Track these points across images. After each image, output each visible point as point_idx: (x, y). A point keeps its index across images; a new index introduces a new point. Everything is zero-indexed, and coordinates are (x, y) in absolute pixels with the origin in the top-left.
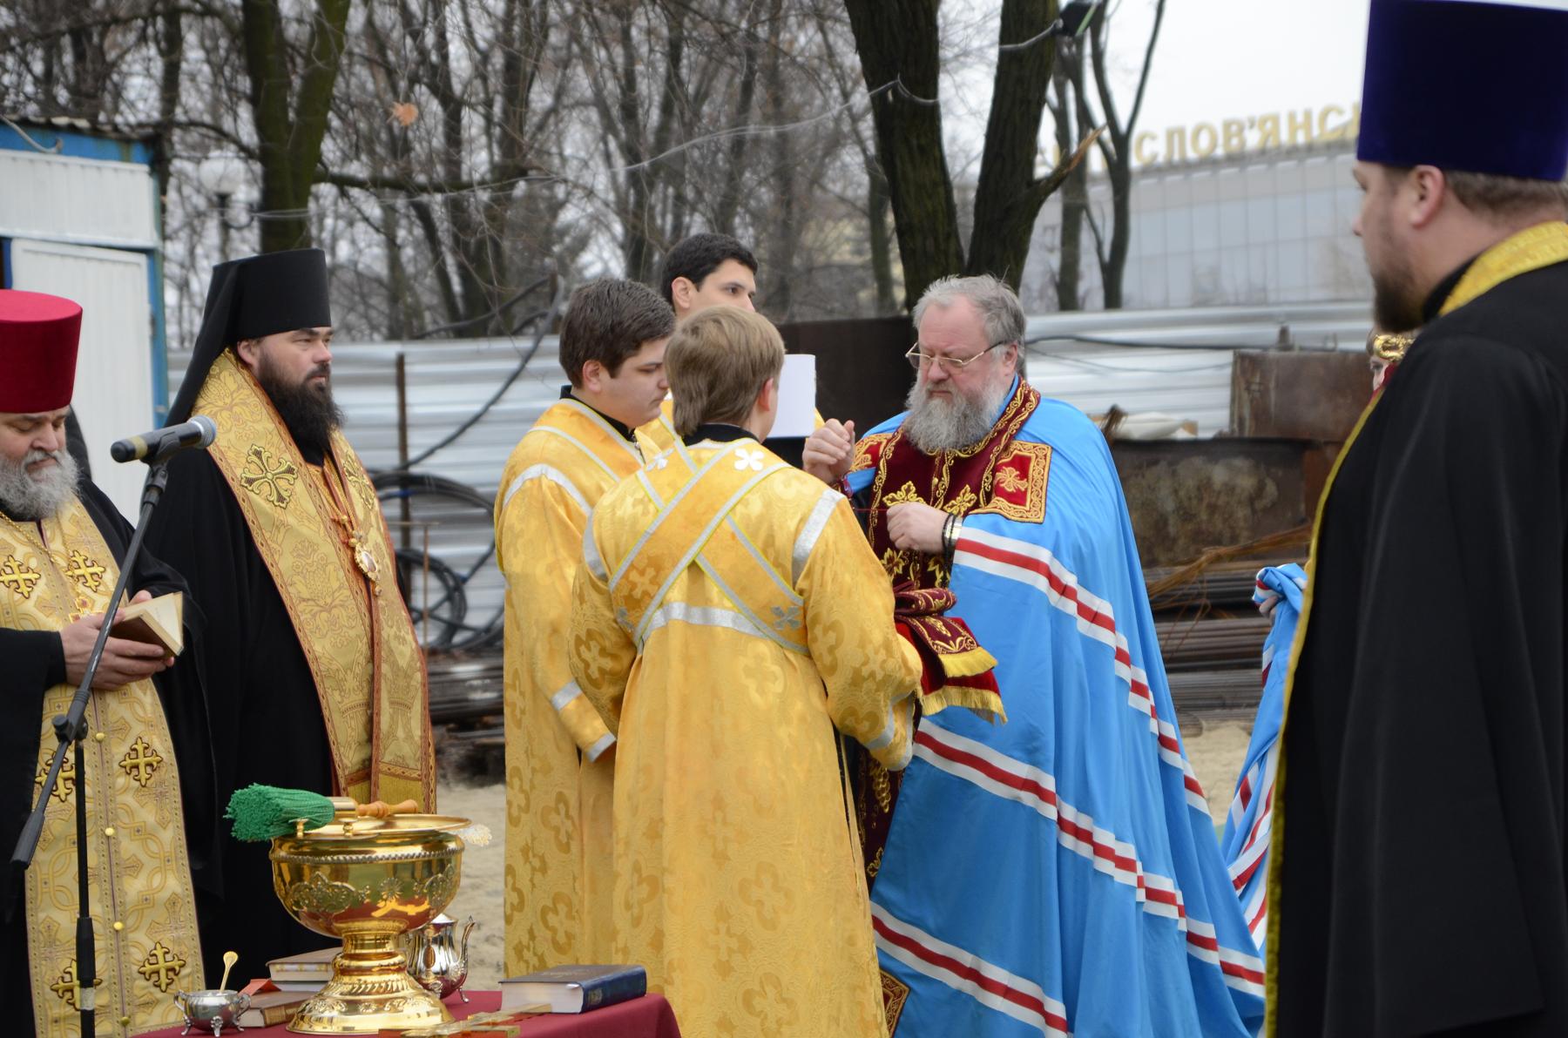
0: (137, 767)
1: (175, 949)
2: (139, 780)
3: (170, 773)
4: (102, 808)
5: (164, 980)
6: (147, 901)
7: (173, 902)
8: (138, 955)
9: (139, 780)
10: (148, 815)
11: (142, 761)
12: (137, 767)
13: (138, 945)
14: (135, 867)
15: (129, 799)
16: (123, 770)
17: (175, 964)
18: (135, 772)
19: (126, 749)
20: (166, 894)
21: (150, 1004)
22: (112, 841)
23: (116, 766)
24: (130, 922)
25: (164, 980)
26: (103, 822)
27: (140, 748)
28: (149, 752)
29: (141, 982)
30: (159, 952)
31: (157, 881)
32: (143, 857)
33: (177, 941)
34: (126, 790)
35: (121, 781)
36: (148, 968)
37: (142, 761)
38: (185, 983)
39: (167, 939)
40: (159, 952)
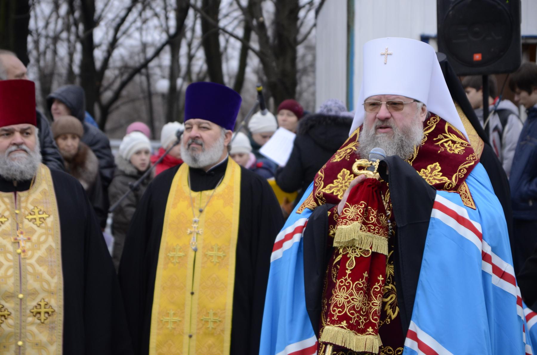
0: (39, 313)
2: (40, 320)
3: (59, 318)
4: (18, 331)
9: (40, 320)
10: (43, 337)
11: (43, 310)
12: (39, 313)
15: (34, 329)
16: (32, 314)
18: (38, 315)
19: (34, 303)
22: (22, 348)
23: (28, 312)
26: (18, 338)
27: (43, 304)
28: (47, 306)
34: (32, 324)
35: (30, 319)
37: (43, 310)
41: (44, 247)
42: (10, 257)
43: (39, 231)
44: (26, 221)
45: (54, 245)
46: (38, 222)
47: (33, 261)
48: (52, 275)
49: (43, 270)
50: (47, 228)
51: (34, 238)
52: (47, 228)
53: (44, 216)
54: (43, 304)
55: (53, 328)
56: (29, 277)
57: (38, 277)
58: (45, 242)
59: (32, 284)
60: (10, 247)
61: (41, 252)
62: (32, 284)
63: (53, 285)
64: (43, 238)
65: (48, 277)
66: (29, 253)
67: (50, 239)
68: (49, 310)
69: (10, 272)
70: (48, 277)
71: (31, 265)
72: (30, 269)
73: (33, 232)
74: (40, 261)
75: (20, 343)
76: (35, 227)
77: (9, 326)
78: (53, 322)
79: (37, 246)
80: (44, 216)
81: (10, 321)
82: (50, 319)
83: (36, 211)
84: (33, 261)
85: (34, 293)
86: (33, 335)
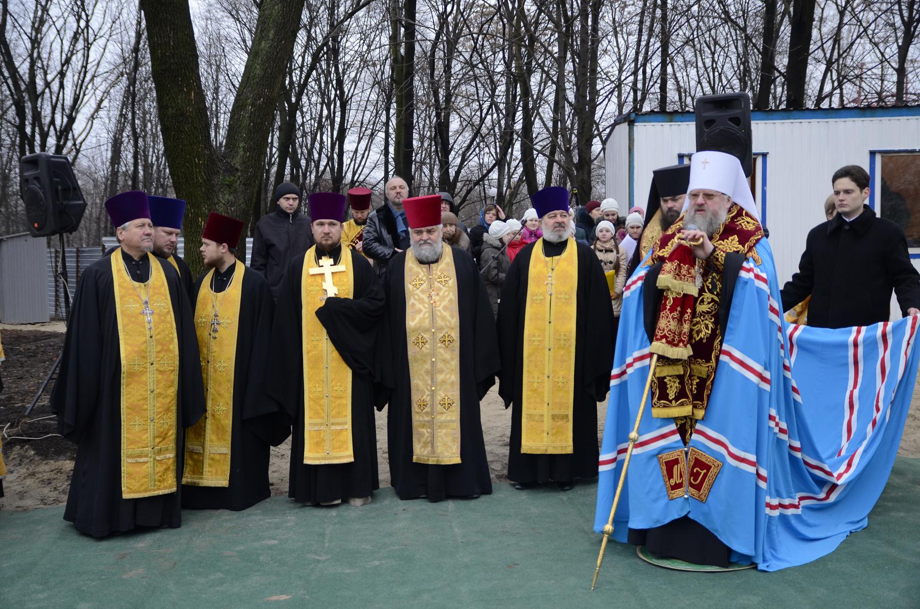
1: (451, 398)
5: (447, 407)
6: (444, 382)
7: (453, 383)
8: (439, 398)
10: (447, 356)
11: (447, 339)
13: (440, 395)
14: (441, 371)
15: (442, 351)
17: (451, 402)
19: (442, 335)
20: (450, 381)
21: (442, 413)
24: (438, 388)
25: (447, 407)
27: (447, 335)
29: (439, 406)
30: (446, 398)
31: (448, 376)
32: (444, 368)
33: (453, 395)
34: (441, 347)
35: (439, 345)
36: (442, 402)
37: (447, 339)
38: (453, 409)
39: (449, 394)
40: (446, 398)
41: (447, 299)
42: (426, 305)
43: (444, 289)
44: (436, 283)
45: (453, 297)
46: (444, 283)
47: (440, 308)
48: (452, 317)
49: (447, 314)
50: (449, 287)
51: (441, 294)
52: (449, 287)
53: (447, 279)
54: (447, 335)
55: (453, 351)
56: (438, 319)
57: (443, 318)
58: (447, 296)
59: (440, 323)
60: (426, 300)
61: (445, 303)
62: (440, 323)
63: (453, 323)
64: (446, 293)
65: (450, 318)
66: (438, 303)
67: (451, 294)
68: (451, 339)
69: (427, 315)
70: (450, 318)
71: (439, 311)
72: (438, 313)
73: (440, 289)
74: (445, 308)
75: (434, 360)
76: (441, 286)
77: (426, 349)
78: (453, 347)
79: (444, 297)
80: (447, 279)
81: (427, 346)
82: (451, 344)
83: (442, 276)
84: (440, 308)
85: (441, 329)
86: (442, 355)
